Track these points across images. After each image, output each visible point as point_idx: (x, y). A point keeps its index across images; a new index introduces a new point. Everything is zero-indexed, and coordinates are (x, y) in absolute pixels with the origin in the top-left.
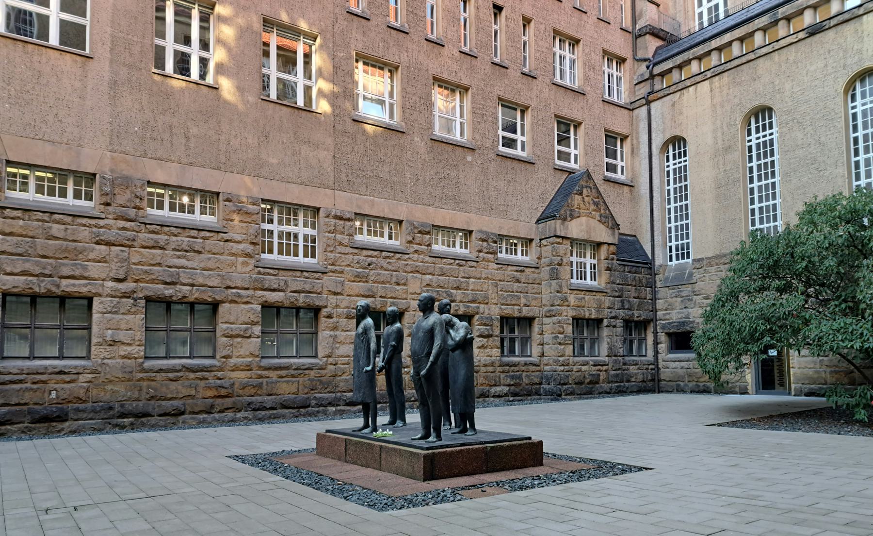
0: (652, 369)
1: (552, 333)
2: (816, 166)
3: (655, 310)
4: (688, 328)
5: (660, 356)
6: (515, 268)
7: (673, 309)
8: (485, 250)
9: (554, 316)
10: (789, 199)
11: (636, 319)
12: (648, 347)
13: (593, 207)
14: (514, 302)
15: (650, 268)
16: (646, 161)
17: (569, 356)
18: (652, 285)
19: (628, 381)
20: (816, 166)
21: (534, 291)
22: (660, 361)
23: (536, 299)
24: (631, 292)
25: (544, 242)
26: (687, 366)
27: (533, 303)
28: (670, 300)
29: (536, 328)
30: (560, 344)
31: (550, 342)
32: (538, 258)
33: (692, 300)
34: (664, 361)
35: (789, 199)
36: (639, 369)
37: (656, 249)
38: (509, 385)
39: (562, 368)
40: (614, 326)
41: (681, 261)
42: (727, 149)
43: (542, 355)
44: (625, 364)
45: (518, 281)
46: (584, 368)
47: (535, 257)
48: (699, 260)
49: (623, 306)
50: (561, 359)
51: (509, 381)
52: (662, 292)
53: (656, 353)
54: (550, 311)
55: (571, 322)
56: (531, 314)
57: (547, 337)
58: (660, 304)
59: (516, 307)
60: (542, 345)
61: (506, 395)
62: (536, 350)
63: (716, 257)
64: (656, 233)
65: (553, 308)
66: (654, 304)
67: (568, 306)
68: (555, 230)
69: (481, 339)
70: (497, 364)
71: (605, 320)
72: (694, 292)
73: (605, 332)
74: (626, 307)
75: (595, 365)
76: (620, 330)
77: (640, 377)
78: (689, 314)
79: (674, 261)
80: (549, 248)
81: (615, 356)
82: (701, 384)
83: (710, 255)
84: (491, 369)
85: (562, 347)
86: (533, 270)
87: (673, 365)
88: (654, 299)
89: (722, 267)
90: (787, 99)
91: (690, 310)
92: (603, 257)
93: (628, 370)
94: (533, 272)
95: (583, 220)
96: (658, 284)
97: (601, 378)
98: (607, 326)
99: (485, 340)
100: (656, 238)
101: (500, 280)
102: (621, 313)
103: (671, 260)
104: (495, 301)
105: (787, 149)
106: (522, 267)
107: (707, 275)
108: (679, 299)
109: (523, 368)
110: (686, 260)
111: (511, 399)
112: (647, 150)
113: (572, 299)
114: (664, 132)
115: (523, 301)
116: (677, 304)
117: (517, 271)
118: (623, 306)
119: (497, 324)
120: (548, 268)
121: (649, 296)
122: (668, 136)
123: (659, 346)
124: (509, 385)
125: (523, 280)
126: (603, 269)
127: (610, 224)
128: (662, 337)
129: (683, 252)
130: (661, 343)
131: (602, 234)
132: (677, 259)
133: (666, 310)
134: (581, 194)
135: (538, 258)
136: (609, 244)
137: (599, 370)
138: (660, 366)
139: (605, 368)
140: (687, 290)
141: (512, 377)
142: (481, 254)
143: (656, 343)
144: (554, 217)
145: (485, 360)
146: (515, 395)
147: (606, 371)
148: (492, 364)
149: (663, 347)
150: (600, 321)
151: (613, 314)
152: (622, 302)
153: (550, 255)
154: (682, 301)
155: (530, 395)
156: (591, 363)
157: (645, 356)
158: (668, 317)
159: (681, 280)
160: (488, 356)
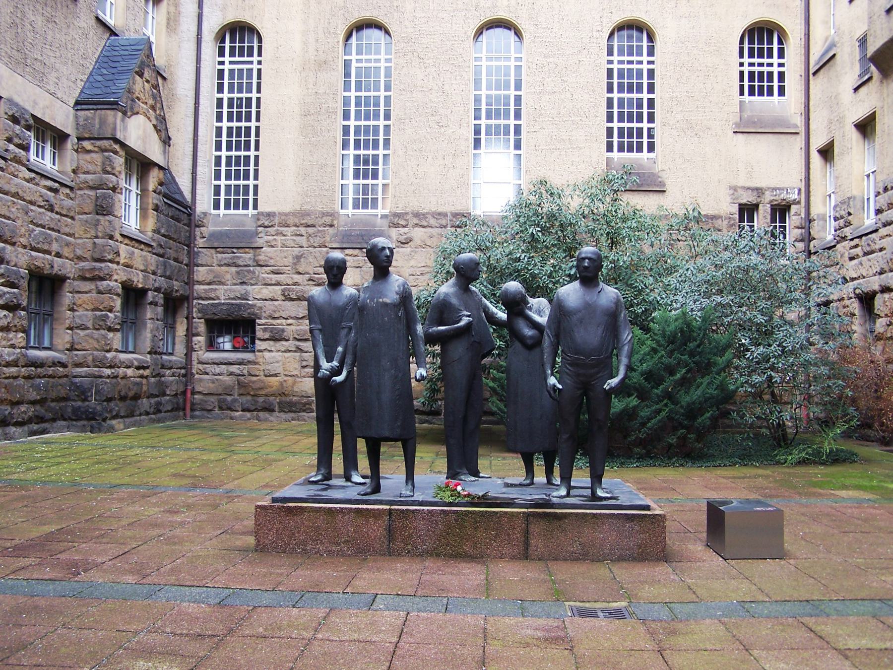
0: (184, 376)
1: (96, 309)
2: (437, 118)
3: (190, 282)
4: (245, 315)
5: (194, 356)
6: (49, 183)
7: (221, 283)
8: (16, 140)
9: (102, 279)
10: (401, 153)
11: (175, 294)
12: (177, 340)
13: (151, 102)
14: (46, 247)
15: (189, 215)
16: (193, 46)
17: (117, 351)
18: (189, 243)
19: (164, 394)
20: (437, 118)
21: (67, 230)
22: (195, 363)
23: (68, 244)
24: (171, 253)
25: (87, 145)
26: (239, 372)
27: (66, 252)
28: (216, 268)
29: (67, 298)
30: (110, 329)
31: (90, 325)
32: (74, 171)
33: (254, 273)
34: (200, 363)
35: (401, 153)
36: (173, 375)
37: (199, 186)
38: (33, 403)
39: (108, 372)
40: (156, 304)
41: (232, 212)
42: (323, 65)
43: (72, 349)
44: (163, 367)
45: (51, 209)
46: (130, 372)
47: (69, 169)
48: (269, 215)
49: (165, 272)
50: (109, 355)
51: (33, 395)
52: (206, 256)
53: (190, 349)
54: (94, 269)
55: (120, 291)
56: (63, 272)
57: (85, 316)
58: (201, 273)
59: (48, 256)
60: (71, 328)
61: (30, 421)
62: (64, 338)
63: (294, 214)
64: (200, 161)
65: (103, 265)
66: (191, 273)
67: (118, 263)
68: (115, 129)
69: (5, 312)
70: (22, 362)
71: (150, 293)
72: (257, 261)
73: (149, 313)
74: (168, 273)
75: (138, 368)
76: (160, 309)
77: (174, 387)
78: (247, 293)
79: (222, 211)
80: (97, 157)
81: (156, 353)
82: (261, 399)
83: (287, 208)
84: (13, 370)
85: (111, 335)
86: (68, 191)
87: (218, 369)
88: (192, 264)
89: (303, 230)
90: (407, 23)
91: (249, 288)
92: (151, 187)
93: (164, 376)
94: (67, 195)
95: (141, 118)
96: (200, 242)
97: (145, 388)
98: (151, 303)
99: (11, 315)
100: (199, 169)
101: (32, 203)
102: (161, 282)
103: (217, 206)
104: (23, 241)
105: (402, 87)
106: (58, 186)
107: (278, 238)
108: (234, 269)
109: (51, 371)
110: (241, 212)
111: (36, 427)
112: (194, 28)
113: (124, 249)
114: (224, 8)
115: (55, 247)
116: (228, 276)
117: (50, 189)
118: (165, 272)
119: (24, 284)
120: (92, 193)
121: (186, 261)
122: (231, 18)
123: (195, 339)
124: (33, 403)
125: (57, 209)
126: (151, 206)
127: (163, 135)
128: (201, 327)
129: (240, 198)
130: (198, 335)
131: (154, 152)
132: (227, 207)
133: (209, 284)
134: (141, 75)
135: (74, 171)
136: (161, 168)
137: (142, 377)
138: (194, 371)
139: (147, 372)
140: (246, 257)
141: (37, 388)
142: (12, 147)
143: (190, 334)
144: (113, 105)
145: (9, 355)
146: (40, 419)
147: (146, 377)
148: (15, 363)
149: (200, 340)
150: (143, 292)
151: (157, 285)
152: (165, 265)
153: (99, 169)
154: (238, 273)
155: (54, 420)
156: (136, 363)
157: (172, 354)
158: (213, 295)
159: (235, 243)
160: (13, 346)
